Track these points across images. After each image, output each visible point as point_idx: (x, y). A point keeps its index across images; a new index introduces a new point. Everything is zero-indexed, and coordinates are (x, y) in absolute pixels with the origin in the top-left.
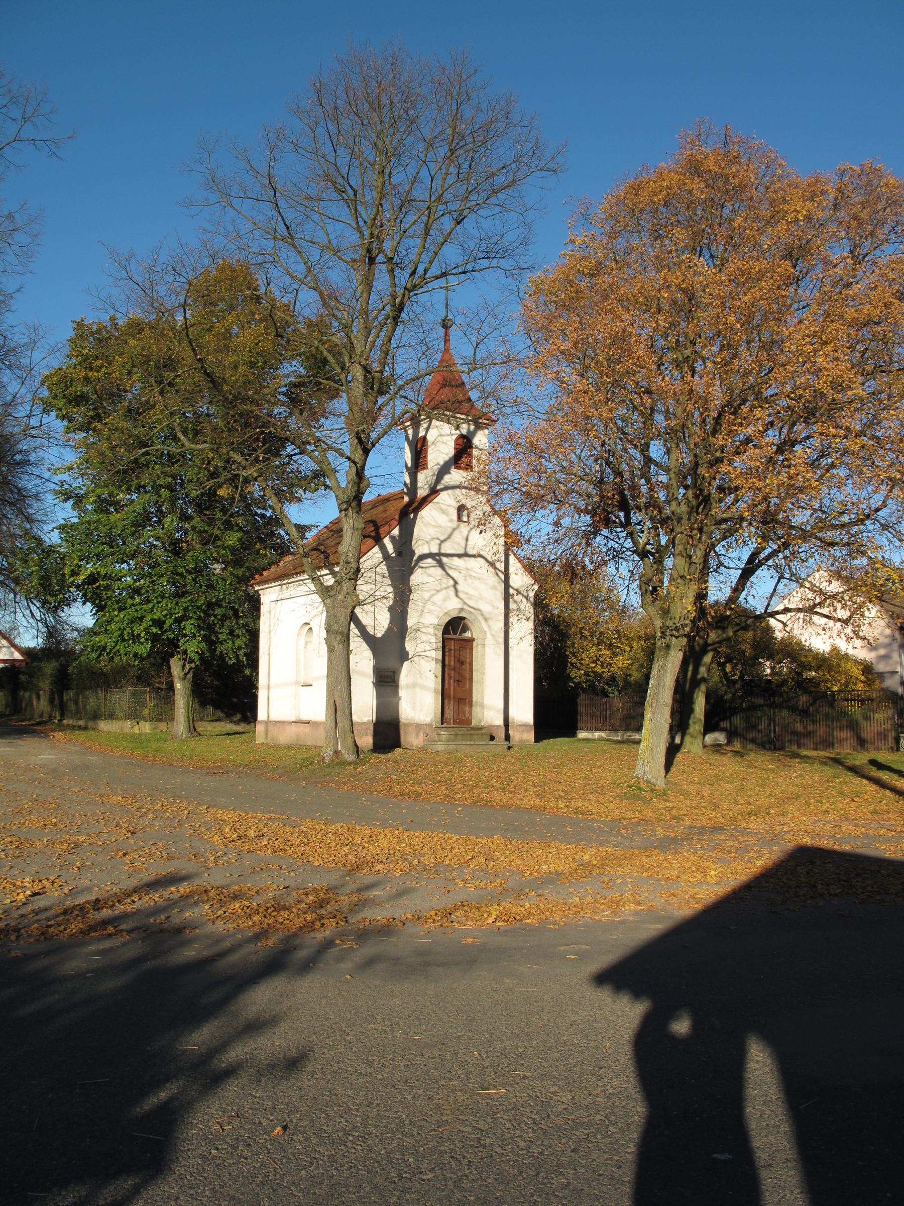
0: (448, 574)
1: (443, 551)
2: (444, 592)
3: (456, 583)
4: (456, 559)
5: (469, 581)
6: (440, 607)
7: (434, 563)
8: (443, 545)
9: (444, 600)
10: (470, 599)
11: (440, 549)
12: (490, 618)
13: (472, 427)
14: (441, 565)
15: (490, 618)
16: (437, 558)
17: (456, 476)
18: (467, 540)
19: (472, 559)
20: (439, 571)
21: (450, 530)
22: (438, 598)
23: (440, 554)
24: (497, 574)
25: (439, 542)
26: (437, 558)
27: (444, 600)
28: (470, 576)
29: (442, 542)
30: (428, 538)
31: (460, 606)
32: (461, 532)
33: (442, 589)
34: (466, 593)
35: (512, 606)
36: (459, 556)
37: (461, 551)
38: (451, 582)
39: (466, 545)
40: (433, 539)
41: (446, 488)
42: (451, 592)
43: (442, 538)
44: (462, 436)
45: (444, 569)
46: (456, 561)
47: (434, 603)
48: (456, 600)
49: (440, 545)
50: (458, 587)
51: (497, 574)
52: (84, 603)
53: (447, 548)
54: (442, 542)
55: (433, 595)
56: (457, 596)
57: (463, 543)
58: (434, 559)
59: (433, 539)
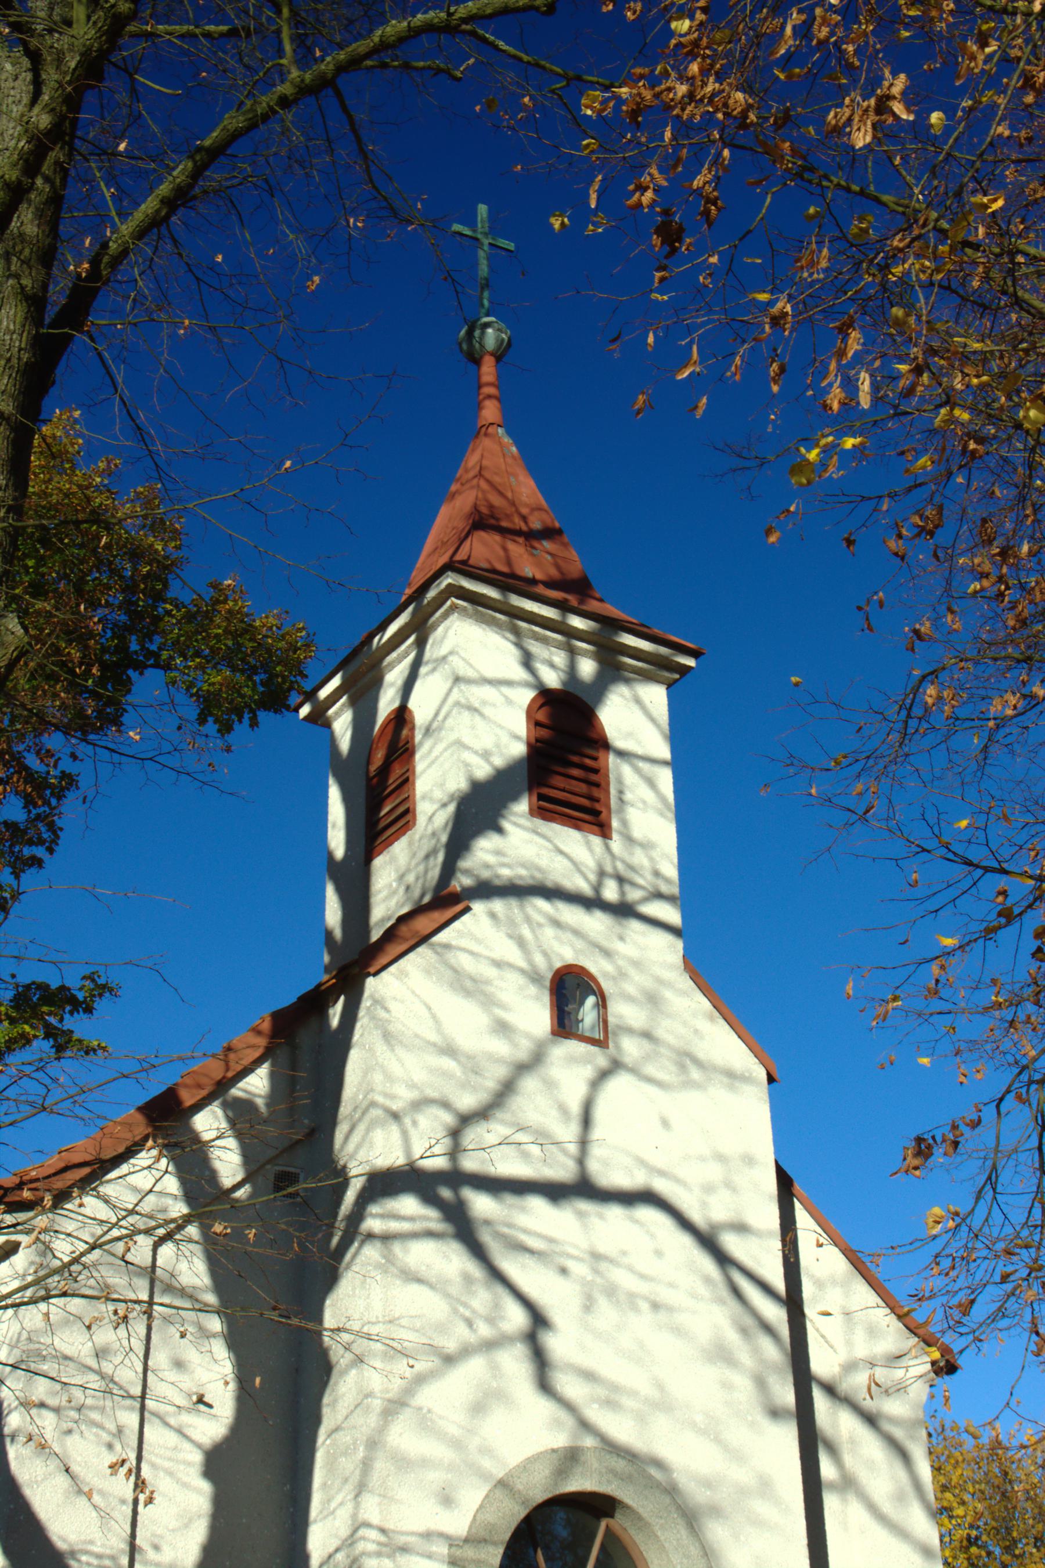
0: (497, 1275)
1: (470, 1164)
2: (476, 1366)
3: (539, 1319)
4: (537, 1203)
5: (606, 1313)
6: (457, 1444)
7: (430, 1217)
8: (472, 1136)
9: (478, 1409)
10: (610, 1404)
11: (455, 1152)
12: (716, 1511)
13: (587, 668)
14: (464, 1229)
15: (716, 1511)
16: (445, 1191)
17: (523, 842)
18: (587, 1120)
19: (615, 1212)
20: (449, 1260)
21: (501, 1072)
22: (447, 1395)
23: (456, 1178)
24: (736, 1292)
25: (448, 1119)
26: (445, 1191)
27: (478, 1409)
28: (611, 1291)
29: (466, 1120)
30: (404, 1095)
31: (560, 1440)
32: (550, 1085)
33: (466, 1352)
34: (589, 1376)
35: (827, 1470)
36: (555, 1192)
37: (562, 1171)
38: (516, 1318)
39: (584, 1143)
40: (420, 1104)
41: (486, 890)
42: (515, 1363)
43: (467, 1101)
44: (546, 697)
45: (478, 1251)
46: (537, 1216)
47: (426, 1423)
48: (543, 1407)
49: (455, 1134)
50: (555, 1344)
51: (736, 1292)
52: (52, 1047)
53: (493, 1152)
54: (466, 1120)
55: (420, 1380)
56: (544, 1385)
57: (568, 1133)
58: (429, 1198)
59: (420, 1104)
